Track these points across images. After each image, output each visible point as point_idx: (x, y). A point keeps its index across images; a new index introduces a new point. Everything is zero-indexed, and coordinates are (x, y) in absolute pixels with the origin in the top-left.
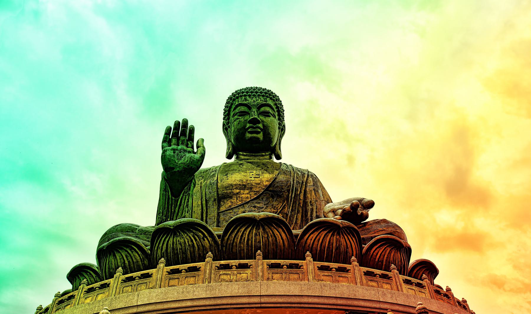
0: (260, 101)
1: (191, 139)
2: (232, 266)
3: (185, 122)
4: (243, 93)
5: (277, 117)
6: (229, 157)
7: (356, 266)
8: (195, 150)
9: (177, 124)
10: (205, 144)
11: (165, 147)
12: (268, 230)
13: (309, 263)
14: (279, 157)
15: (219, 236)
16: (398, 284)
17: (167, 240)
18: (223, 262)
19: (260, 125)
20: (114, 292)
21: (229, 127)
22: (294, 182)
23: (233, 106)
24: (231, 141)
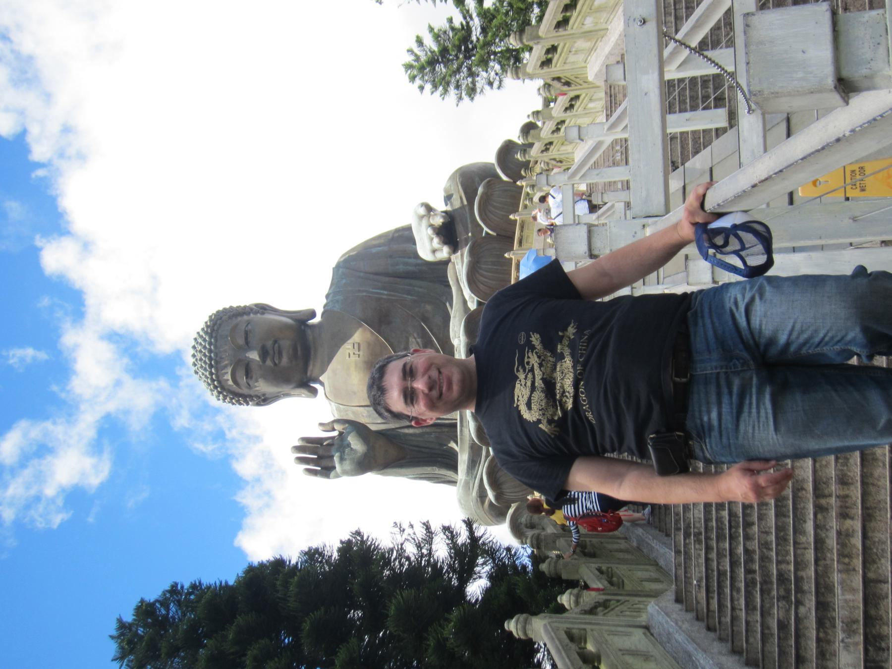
1: (319, 441)
4: (211, 374)
5: (245, 317)
6: (314, 392)
11: (337, 473)
14: (313, 314)
19: (269, 344)
21: (264, 395)
22: (363, 291)
23: (235, 388)
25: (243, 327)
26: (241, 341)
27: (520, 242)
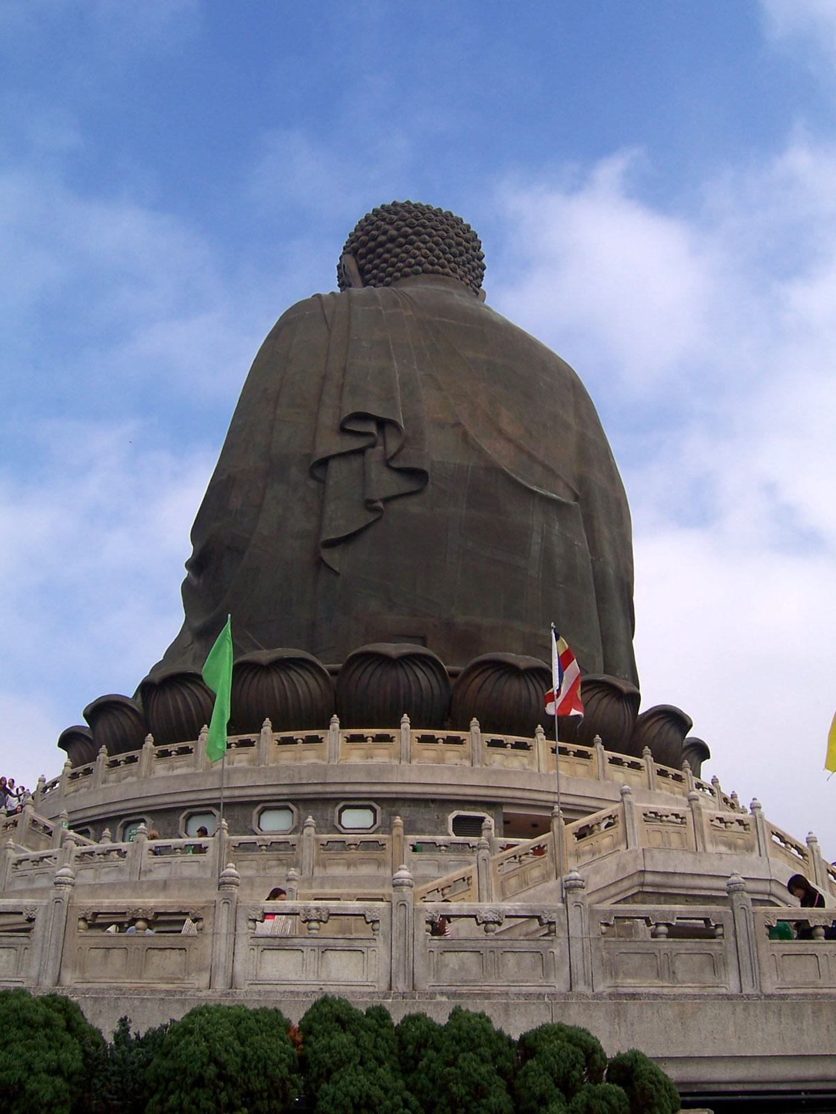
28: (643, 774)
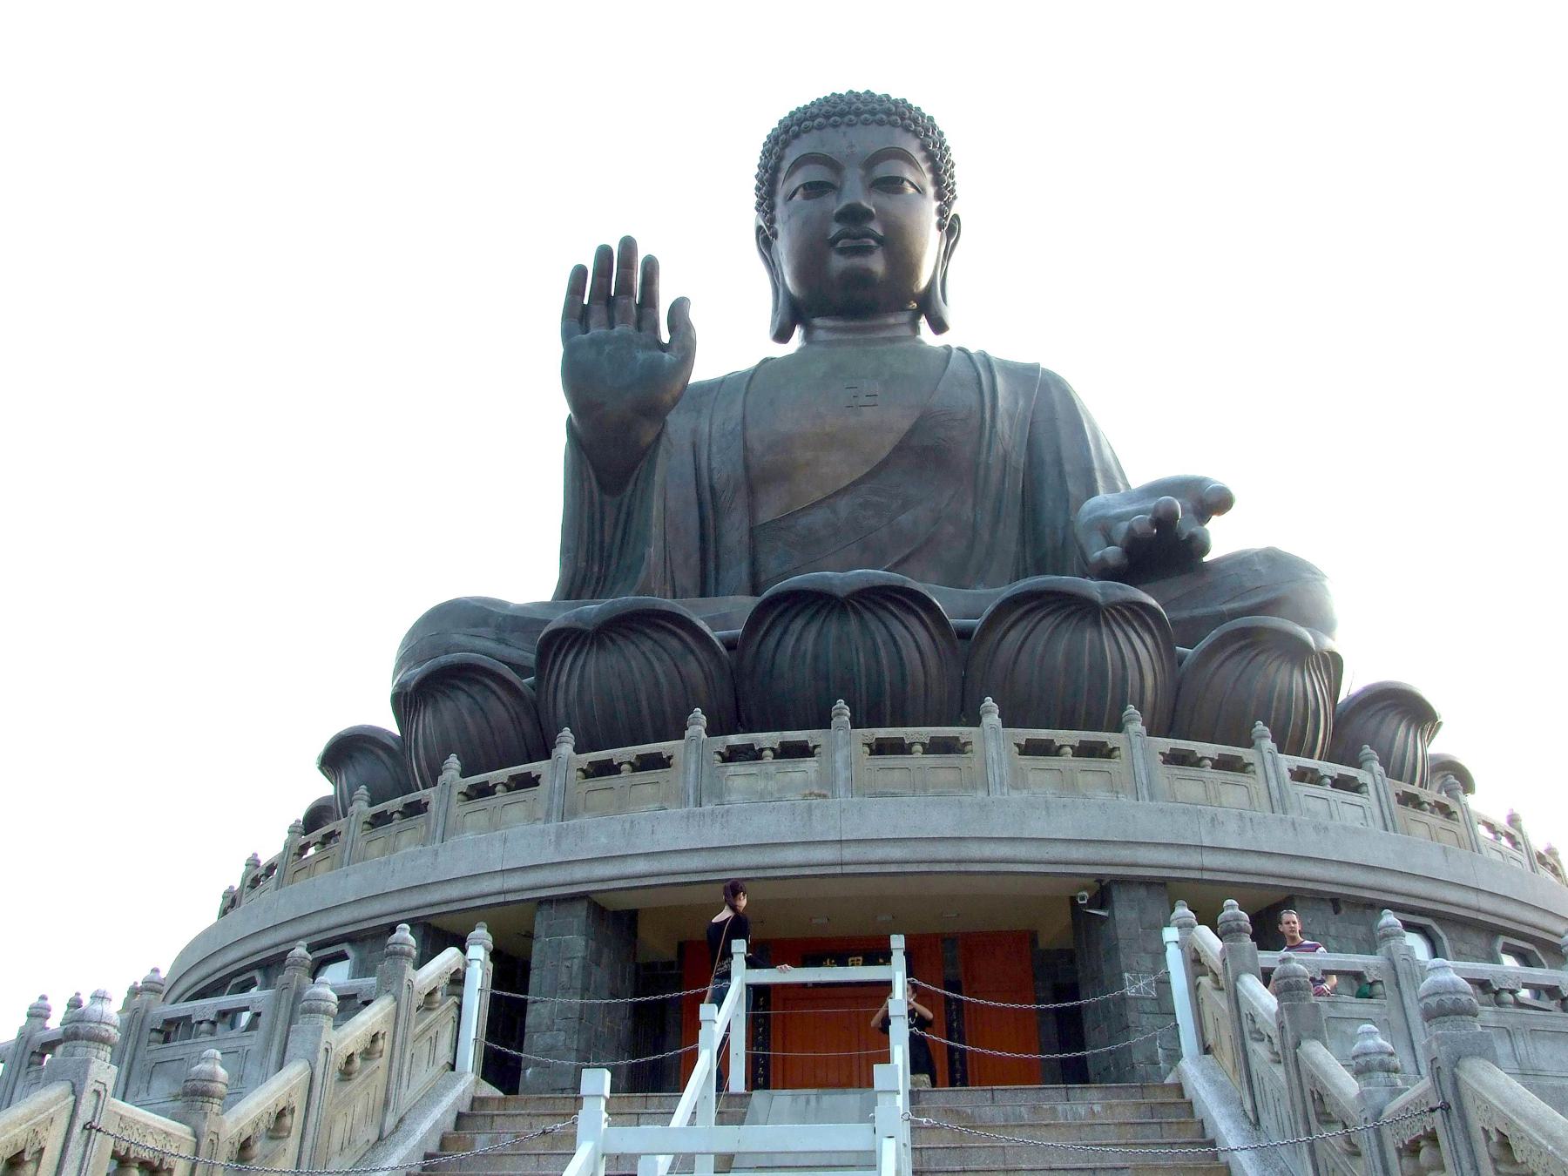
0: (870, 140)
2: (762, 750)
3: (628, 245)
4: (813, 117)
5: (931, 191)
6: (782, 335)
7: (1138, 734)
8: (665, 337)
9: (604, 254)
10: (695, 316)
12: (874, 624)
13: (991, 736)
14: (939, 326)
15: (730, 645)
16: (1273, 783)
17: (580, 662)
18: (735, 739)
20: (439, 832)
21: (775, 235)
23: (786, 165)
24: (784, 284)
25: (909, 174)
26: (881, 171)
27: (1177, 759)
28: (1369, 800)
